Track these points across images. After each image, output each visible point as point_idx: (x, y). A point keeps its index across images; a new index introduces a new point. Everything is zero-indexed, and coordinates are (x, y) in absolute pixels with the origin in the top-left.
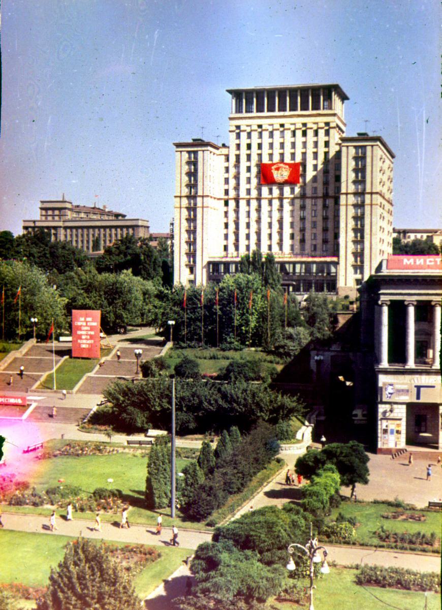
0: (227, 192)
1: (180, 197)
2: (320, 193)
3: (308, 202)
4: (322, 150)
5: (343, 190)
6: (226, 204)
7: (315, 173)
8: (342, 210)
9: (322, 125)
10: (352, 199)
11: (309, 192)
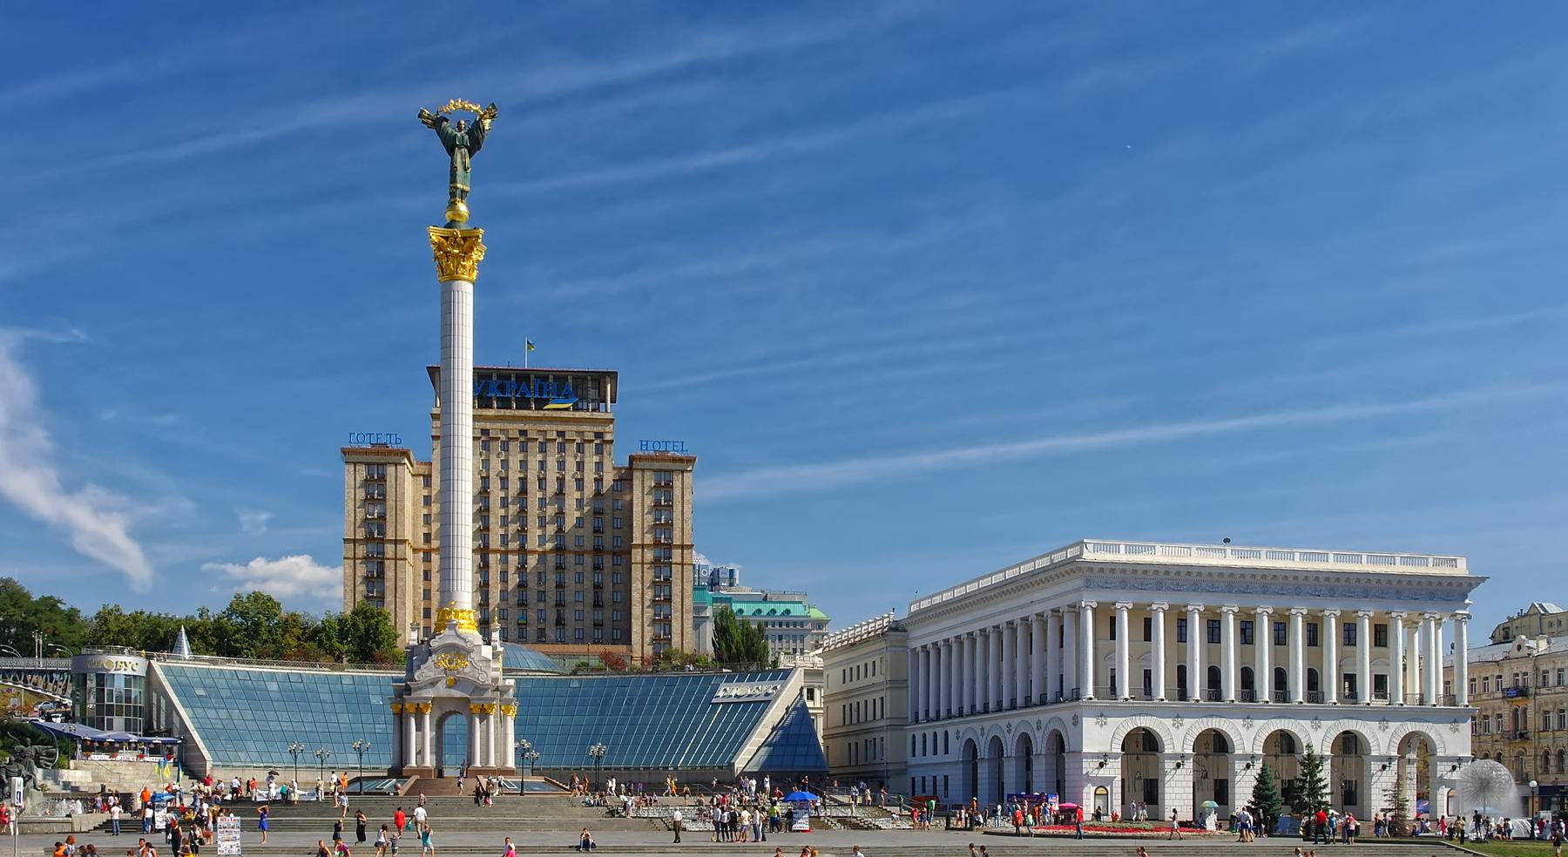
0: (427, 537)
1: (354, 541)
2: (589, 545)
3: (570, 559)
4: (589, 476)
5: (637, 541)
6: (427, 559)
7: (578, 514)
9: (590, 436)
11: (570, 543)
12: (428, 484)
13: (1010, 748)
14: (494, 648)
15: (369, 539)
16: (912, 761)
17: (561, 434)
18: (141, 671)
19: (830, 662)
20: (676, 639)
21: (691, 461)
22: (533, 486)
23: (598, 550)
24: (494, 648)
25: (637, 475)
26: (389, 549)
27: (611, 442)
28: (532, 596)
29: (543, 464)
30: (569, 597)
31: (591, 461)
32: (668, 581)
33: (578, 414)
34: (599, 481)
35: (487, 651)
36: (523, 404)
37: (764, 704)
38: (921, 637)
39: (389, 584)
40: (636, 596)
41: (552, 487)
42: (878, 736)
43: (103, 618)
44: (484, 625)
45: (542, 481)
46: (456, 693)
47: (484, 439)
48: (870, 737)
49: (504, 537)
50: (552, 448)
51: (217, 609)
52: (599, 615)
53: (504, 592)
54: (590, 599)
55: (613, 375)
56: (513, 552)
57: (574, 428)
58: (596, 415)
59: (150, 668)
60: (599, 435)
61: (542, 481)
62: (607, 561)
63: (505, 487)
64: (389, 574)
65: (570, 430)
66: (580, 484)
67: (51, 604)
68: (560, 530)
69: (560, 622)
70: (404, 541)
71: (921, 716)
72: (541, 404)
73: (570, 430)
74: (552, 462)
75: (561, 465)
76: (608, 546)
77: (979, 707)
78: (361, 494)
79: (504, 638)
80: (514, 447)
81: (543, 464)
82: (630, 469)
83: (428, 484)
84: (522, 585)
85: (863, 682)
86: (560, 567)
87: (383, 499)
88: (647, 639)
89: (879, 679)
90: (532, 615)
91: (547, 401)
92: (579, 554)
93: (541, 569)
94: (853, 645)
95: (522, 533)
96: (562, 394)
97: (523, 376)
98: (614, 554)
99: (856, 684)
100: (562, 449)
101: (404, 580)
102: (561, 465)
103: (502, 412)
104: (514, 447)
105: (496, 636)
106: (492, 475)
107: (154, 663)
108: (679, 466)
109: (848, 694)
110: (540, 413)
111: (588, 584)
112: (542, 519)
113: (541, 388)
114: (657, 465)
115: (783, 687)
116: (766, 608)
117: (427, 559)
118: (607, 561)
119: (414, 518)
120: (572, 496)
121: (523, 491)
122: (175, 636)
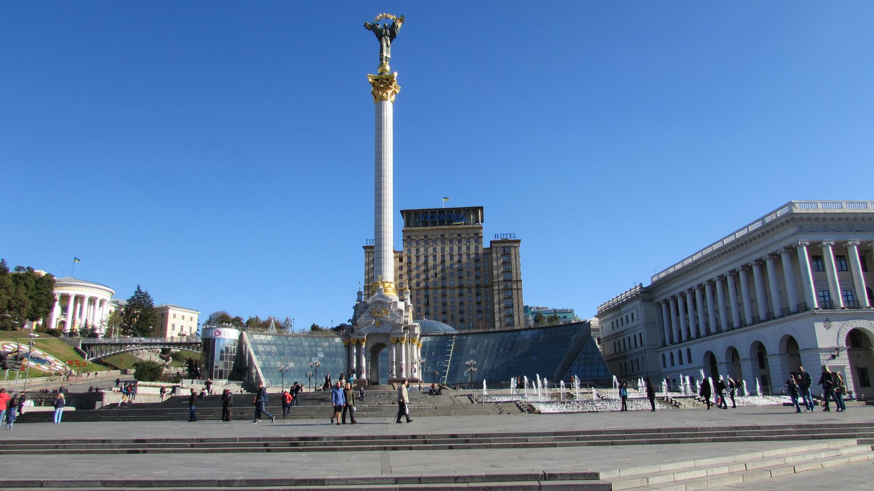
3: (465, 291)
11: (465, 282)
12: (401, 260)
13: (745, 352)
14: (406, 304)
16: (663, 370)
20: (516, 323)
21: (519, 241)
23: (478, 286)
25: (494, 249)
35: (401, 305)
36: (442, 223)
44: (400, 292)
60: (476, 234)
62: (482, 290)
63: (435, 260)
71: (667, 341)
72: (450, 222)
76: (483, 284)
77: (713, 329)
83: (401, 260)
85: (626, 326)
91: (452, 221)
92: (469, 288)
97: (442, 211)
100: (460, 242)
105: (408, 297)
107: (244, 333)
109: (616, 335)
114: (503, 245)
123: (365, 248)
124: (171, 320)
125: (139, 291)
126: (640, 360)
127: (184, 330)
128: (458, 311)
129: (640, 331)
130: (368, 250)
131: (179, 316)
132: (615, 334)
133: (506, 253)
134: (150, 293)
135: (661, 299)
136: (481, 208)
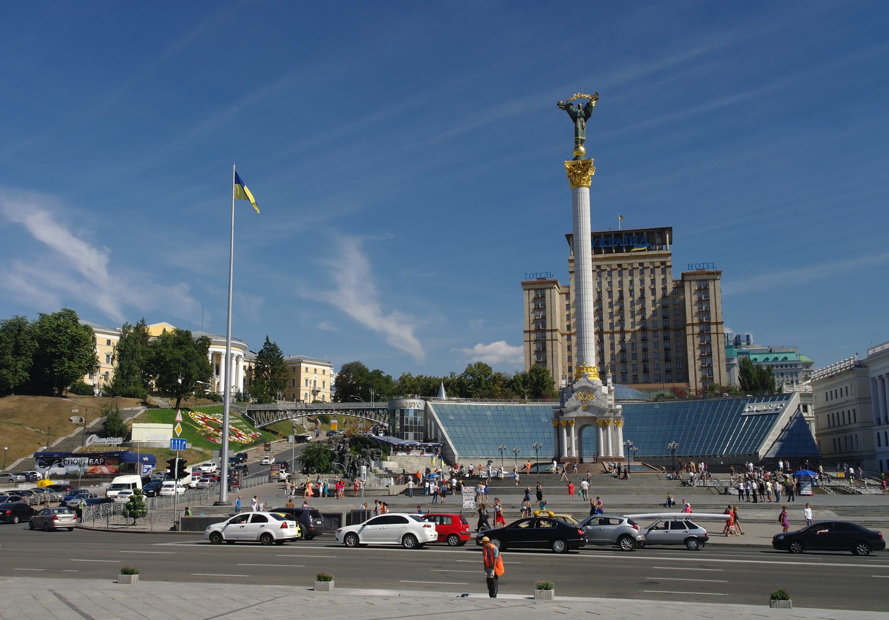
0: (569, 327)
1: (530, 332)
2: (660, 325)
3: (650, 335)
5: (689, 321)
6: (569, 339)
7: (653, 309)
8: (689, 339)
10: (697, 330)
11: (650, 326)
12: (568, 298)
14: (609, 388)
15: (537, 330)
16: (878, 449)
17: (641, 264)
18: (422, 407)
19: (816, 388)
21: (719, 273)
22: (626, 294)
23: (666, 328)
24: (609, 388)
25: (687, 284)
26: (548, 335)
27: (670, 266)
28: (629, 356)
29: (631, 282)
30: (650, 356)
31: (659, 278)
32: (709, 344)
33: (650, 253)
34: (664, 289)
35: (605, 390)
36: (620, 250)
37: (776, 415)
38: (877, 370)
39: (549, 354)
40: (690, 353)
41: (637, 294)
42: (853, 434)
43: (403, 380)
44: (602, 375)
45: (631, 292)
46: (589, 414)
47: (598, 271)
48: (848, 435)
49: (611, 324)
50: (637, 273)
51: (459, 371)
52: (668, 366)
53: (612, 355)
54: (663, 357)
55: (670, 229)
56: (617, 332)
57: (649, 260)
58: (661, 252)
59: (426, 405)
60: (663, 263)
61: (631, 292)
62: (672, 334)
63: (610, 296)
64: (549, 348)
65: (647, 262)
66: (653, 291)
67: (378, 373)
68: (643, 318)
69: (646, 371)
70: (556, 330)
72: (629, 249)
73: (647, 262)
74: (637, 281)
75: (642, 282)
76: (672, 325)
78: (532, 306)
79: (614, 382)
80: (615, 274)
81: (631, 282)
82: (683, 281)
83: (568, 298)
84: (623, 351)
85: (840, 400)
86: (644, 340)
87: (544, 308)
88: (699, 379)
89: (851, 397)
90: (629, 367)
91: (632, 247)
92: (655, 331)
93: (634, 341)
94: (831, 377)
95: (622, 322)
96: (640, 242)
97: (618, 234)
98: (675, 330)
99: (835, 401)
100: (642, 273)
101: (557, 351)
102: (642, 282)
103: (608, 255)
104: (615, 274)
105: (609, 380)
106: (603, 290)
107: (429, 403)
108: (711, 277)
109: (830, 408)
110: (629, 254)
111: (661, 348)
112: (632, 312)
113: (629, 240)
114: (698, 277)
115: (787, 405)
116: (771, 357)
117: (569, 339)
118: (672, 334)
119: (561, 317)
120: (649, 298)
121: (621, 298)
122: (439, 388)
123: (523, 284)
124: (304, 376)
125: (268, 343)
126: (854, 437)
127: (317, 386)
128: (641, 360)
129: (854, 407)
130: (528, 287)
131: (311, 370)
132: (829, 406)
133: (703, 290)
134: (280, 346)
135: (875, 375)
136: (670, 229)
